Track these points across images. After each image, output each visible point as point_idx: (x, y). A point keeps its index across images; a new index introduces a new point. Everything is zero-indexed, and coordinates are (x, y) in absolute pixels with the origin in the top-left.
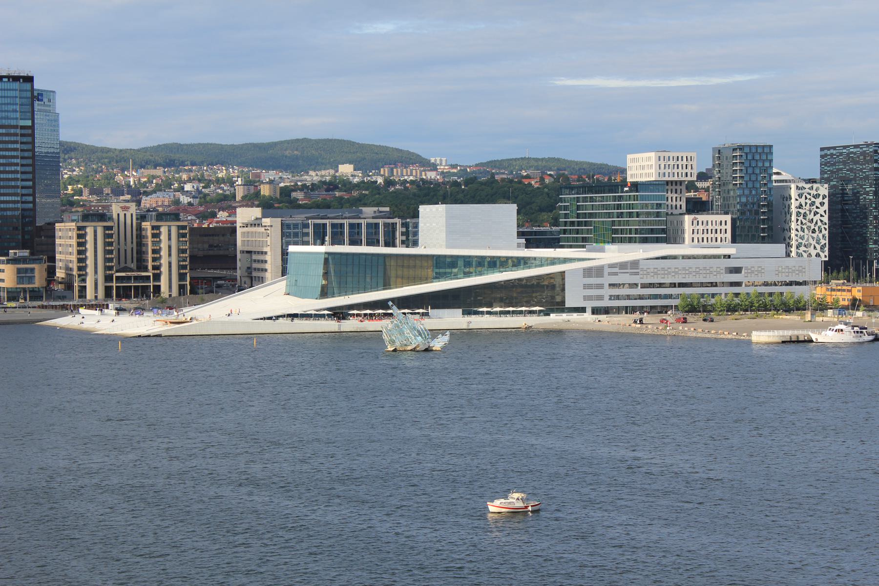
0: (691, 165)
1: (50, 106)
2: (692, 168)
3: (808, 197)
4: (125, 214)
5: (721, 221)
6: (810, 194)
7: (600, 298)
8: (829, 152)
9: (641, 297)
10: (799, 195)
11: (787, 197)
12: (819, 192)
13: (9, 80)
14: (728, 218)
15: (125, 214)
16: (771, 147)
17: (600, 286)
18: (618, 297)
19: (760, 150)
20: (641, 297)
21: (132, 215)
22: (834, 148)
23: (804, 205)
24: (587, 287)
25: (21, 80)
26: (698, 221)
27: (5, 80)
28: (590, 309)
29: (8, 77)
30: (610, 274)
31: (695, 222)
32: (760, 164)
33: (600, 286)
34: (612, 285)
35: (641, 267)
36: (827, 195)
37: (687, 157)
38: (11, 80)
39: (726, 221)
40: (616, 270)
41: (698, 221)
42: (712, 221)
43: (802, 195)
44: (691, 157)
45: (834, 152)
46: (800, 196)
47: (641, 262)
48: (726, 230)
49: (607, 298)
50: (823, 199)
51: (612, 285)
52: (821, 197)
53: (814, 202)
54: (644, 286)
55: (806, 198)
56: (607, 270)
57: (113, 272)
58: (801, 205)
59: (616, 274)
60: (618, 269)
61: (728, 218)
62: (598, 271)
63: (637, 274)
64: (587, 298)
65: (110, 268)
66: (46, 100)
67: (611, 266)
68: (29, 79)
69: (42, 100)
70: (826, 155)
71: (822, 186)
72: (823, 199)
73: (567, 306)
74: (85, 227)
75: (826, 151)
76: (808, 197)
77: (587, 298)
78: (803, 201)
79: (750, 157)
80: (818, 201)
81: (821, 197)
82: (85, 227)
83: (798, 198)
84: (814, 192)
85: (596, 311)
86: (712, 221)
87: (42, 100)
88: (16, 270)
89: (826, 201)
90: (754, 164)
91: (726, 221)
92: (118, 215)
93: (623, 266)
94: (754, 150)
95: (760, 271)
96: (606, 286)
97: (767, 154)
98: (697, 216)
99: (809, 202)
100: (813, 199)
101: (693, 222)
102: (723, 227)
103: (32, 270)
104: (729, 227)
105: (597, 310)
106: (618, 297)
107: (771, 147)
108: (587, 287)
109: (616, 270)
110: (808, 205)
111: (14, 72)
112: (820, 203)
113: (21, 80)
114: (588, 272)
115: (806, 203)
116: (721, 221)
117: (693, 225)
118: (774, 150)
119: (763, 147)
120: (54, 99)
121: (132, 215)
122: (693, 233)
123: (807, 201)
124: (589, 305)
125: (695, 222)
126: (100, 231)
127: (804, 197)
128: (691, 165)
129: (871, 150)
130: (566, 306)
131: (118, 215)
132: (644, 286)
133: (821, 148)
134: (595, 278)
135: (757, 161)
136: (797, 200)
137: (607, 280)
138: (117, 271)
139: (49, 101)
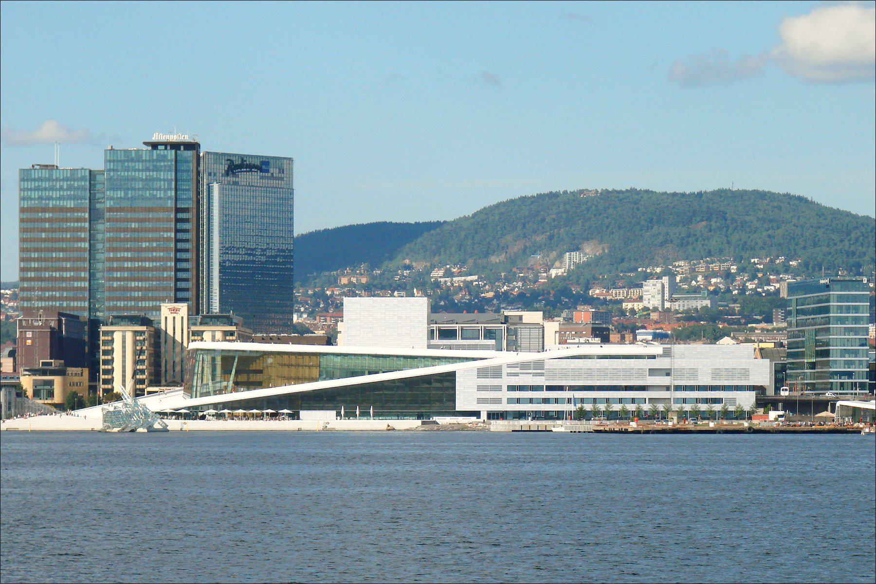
1: (282, 179)
4: (174, 318)
7: (498, 401)
9: (546, 401)
13: (166, 149)
15: (174, 318)
17: (498, 388)
18: (518, 401)
20: (546, 401)
21: (182, 318)
24: (480, 388)
25: (182, 148)
27: (160, 147)
28: (485, 413)
29: (165, 144)
30: (509, 374)
33: (498, 388)
34: (512, 388)
38: (169, 148)
40: (517, 370)
49: (505, 400)
51: (512, 388)
54: (550, 388)
56: (505, 371)
57: (144, 386)
59: (516, 375)
60: (518, 369)
62: (496, 372)
63: (542, 375)
64: (480, 401)
65: (142, 382)
66: (274, 171)
67: (510, 366)
68: (193, 146)
69: (267, 171)
73: (459, 407)
74: (113, 332)
77: (480, 401)
82: (113, 332)
87: (267, 171)
88: (32, 383)
92: (166, 318)
93: (524, 366)
95: (694, 373)
96: (505, 388)
103: (51, 383)
105: (494, 414)
106: (518, 401)
108: (480, 388)
109: (517, 370)
111: (174, 138)
113: (182, 148)
114: (483, 373)
120: (291, 170)
121: (182, 318)
124: (484, 409)
126: (129, 336)
131: (166, 318)
132: (550, 388)
134: (493, 379)
137: (506, 381)
138: (150, 385)
139: (282, 171)
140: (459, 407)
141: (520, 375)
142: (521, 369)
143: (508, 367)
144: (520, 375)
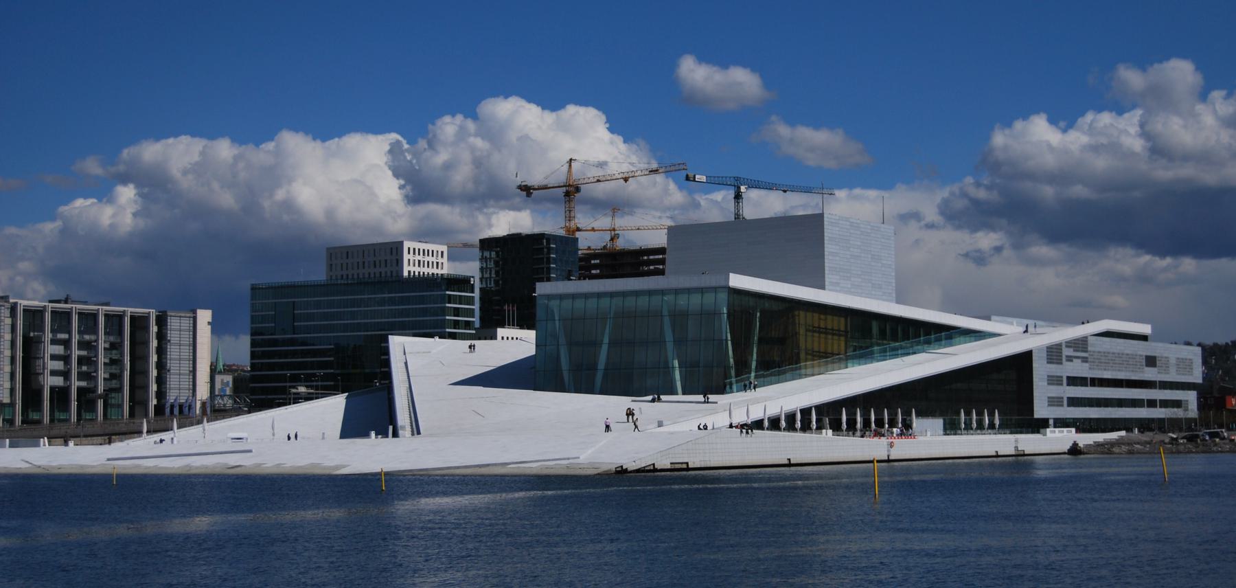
24: (1054, 380)
30: (1070, 359)
34: (1073, 381)
35: (1089, 349)
37: (437, 252)
47: (1090, 338)
51: (1073, 381)
56: (1067, 352)
60: (1072, 350)
63: (1085, 360)
64: (1055, 402)
77: (1055, 402)
85: (1061, 423)
106: (1074, 402)
108: (1054, 380)
130: (1036, 416)
140: (1041, 410)
141: (1074, 360)
142: (1074, 351)
143: (1067, 346)
144: (1074, 360)
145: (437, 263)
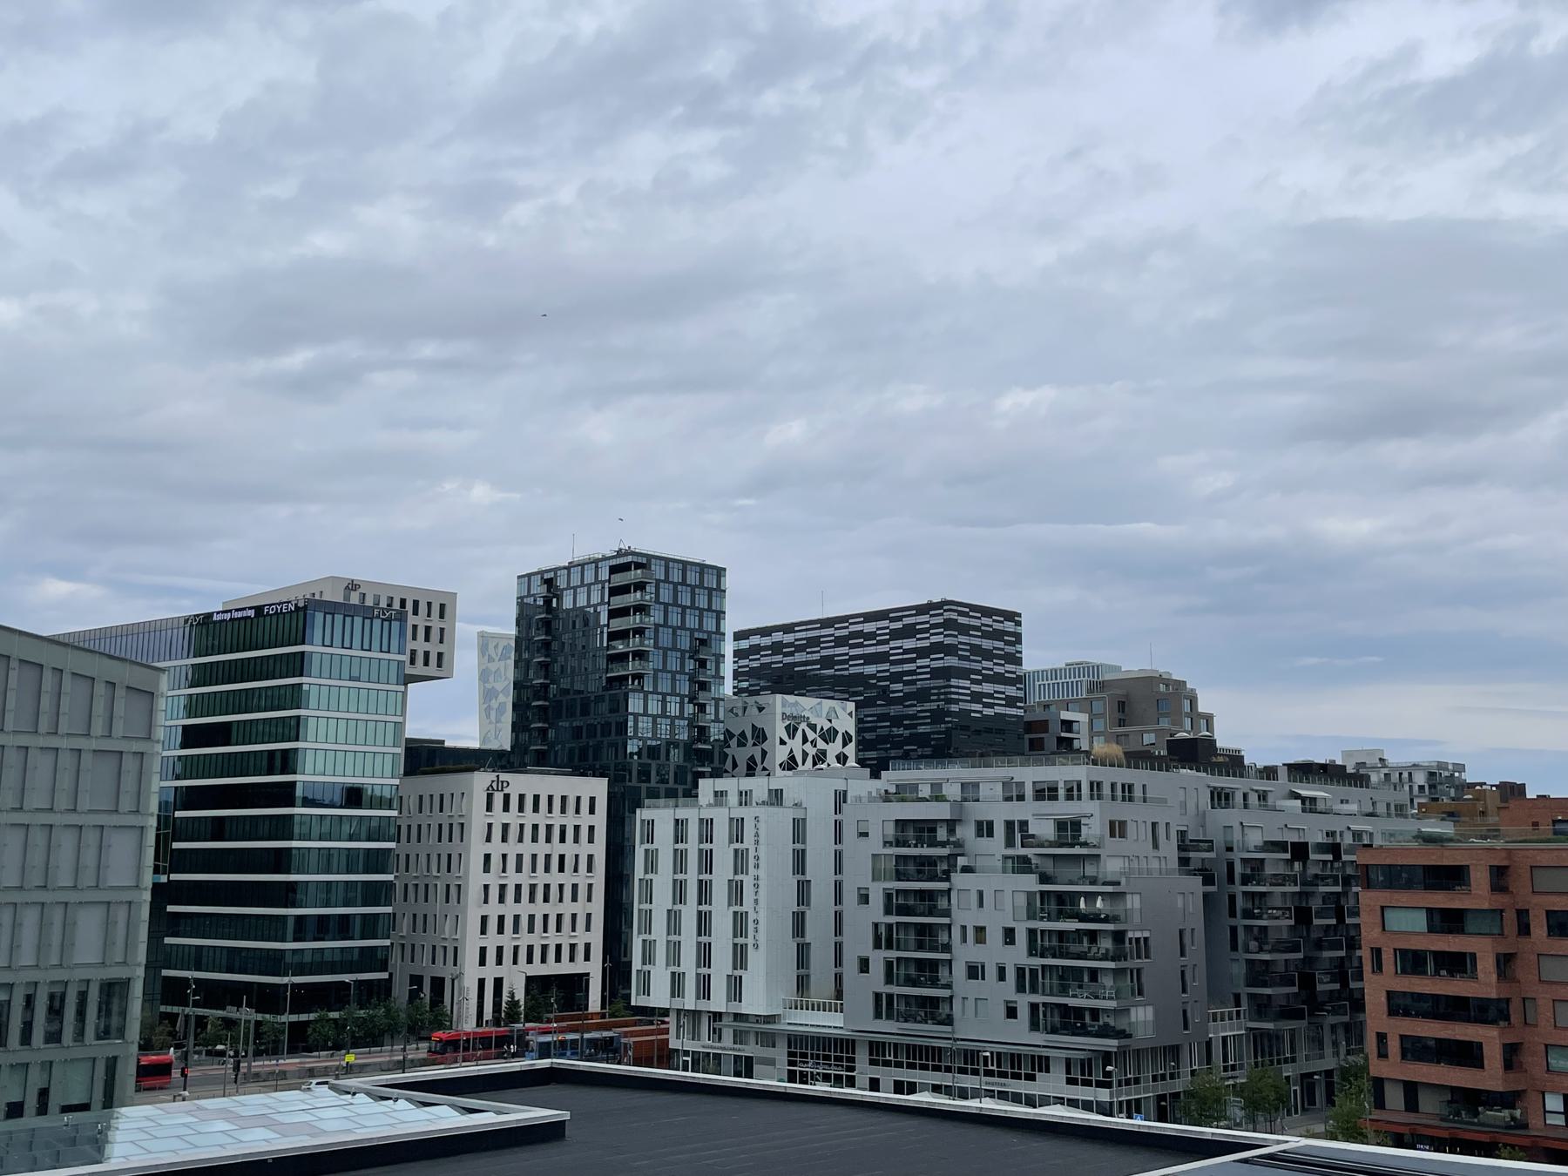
0: (442, 630)
2: (441, 641)
3: (811, 735)
5: (578, 799)
6: (813, 727)
8: (766, 641)
10: (787, 728)
11: (743, 734)
12: (835, 724)
14: (598, 788)
16: (720, 572)
19: (692, 578)
22: (788, 628)
23: (799, 759)
26: (507, 798)
31: (498, 799)
32: (691, 622)
36: (852, 733)
37: (429, 604)
39: (592, 800)
41: (507, 798)
42: (550, 798)
43: (796, 729)
44: (442, 607)
45: (789, 638)
46: (791, 731)
48: (591, 828)
50: (845, 744)
52: (839, 738)
53: (824, 753)
55: (805, 740)
58: (792, 758)
61: (598, 788)
70: (756, 649)
71: (844, 709)
72: (845, 744)
75: (755, 640)
76: (811, 735)
78: (796, 744)
79: (666, 595)
80: (834, 748)
81: (839, 738)
83: (786, 738)
84: (823, 723)
86: (550, 798)
89: (850, 750)
90: (675, 619)
91: (592, 800)
94: (676, 576)
97: (710, 590)
98: (504, 777)
99: (812, 751)
100: (821, 744)
101: (490, 797)
102: (585, 820)
104: (600, 820)
107: (720, 572)
110: (810, 760)
112: (838, 758)
115: (805, 755)
116: (578, 799)
117: (489, 808)
118: (729, 582)
119: (703, 568)
122: (488, 839)
123: (808, 747)
125: (498, 799)
127: (799, 734)
128: (442, 630)
129: (940, 620)
133: (735, 633)
135: (684, 608)
136: (783, 742)
145: (428, 629)
